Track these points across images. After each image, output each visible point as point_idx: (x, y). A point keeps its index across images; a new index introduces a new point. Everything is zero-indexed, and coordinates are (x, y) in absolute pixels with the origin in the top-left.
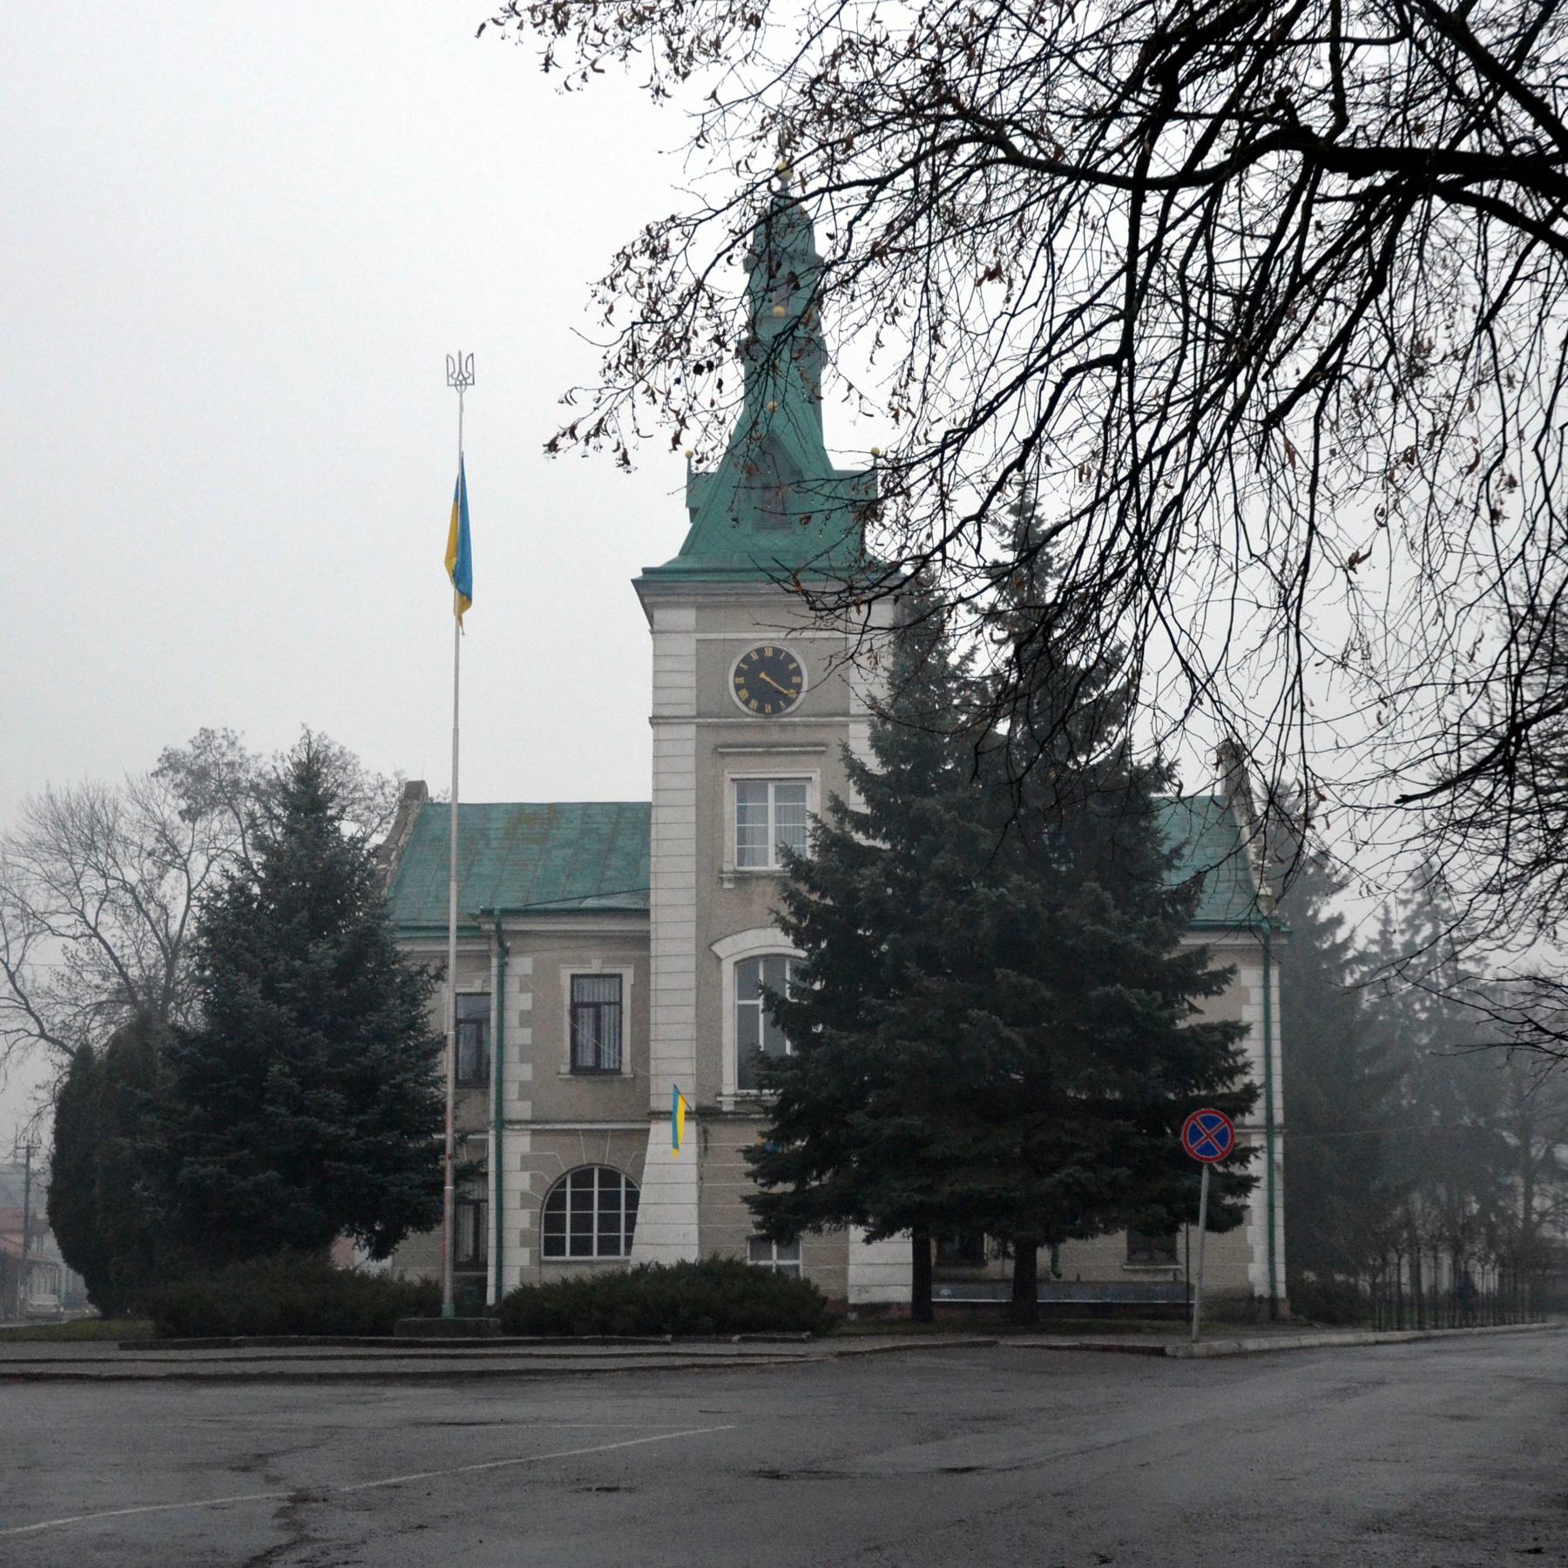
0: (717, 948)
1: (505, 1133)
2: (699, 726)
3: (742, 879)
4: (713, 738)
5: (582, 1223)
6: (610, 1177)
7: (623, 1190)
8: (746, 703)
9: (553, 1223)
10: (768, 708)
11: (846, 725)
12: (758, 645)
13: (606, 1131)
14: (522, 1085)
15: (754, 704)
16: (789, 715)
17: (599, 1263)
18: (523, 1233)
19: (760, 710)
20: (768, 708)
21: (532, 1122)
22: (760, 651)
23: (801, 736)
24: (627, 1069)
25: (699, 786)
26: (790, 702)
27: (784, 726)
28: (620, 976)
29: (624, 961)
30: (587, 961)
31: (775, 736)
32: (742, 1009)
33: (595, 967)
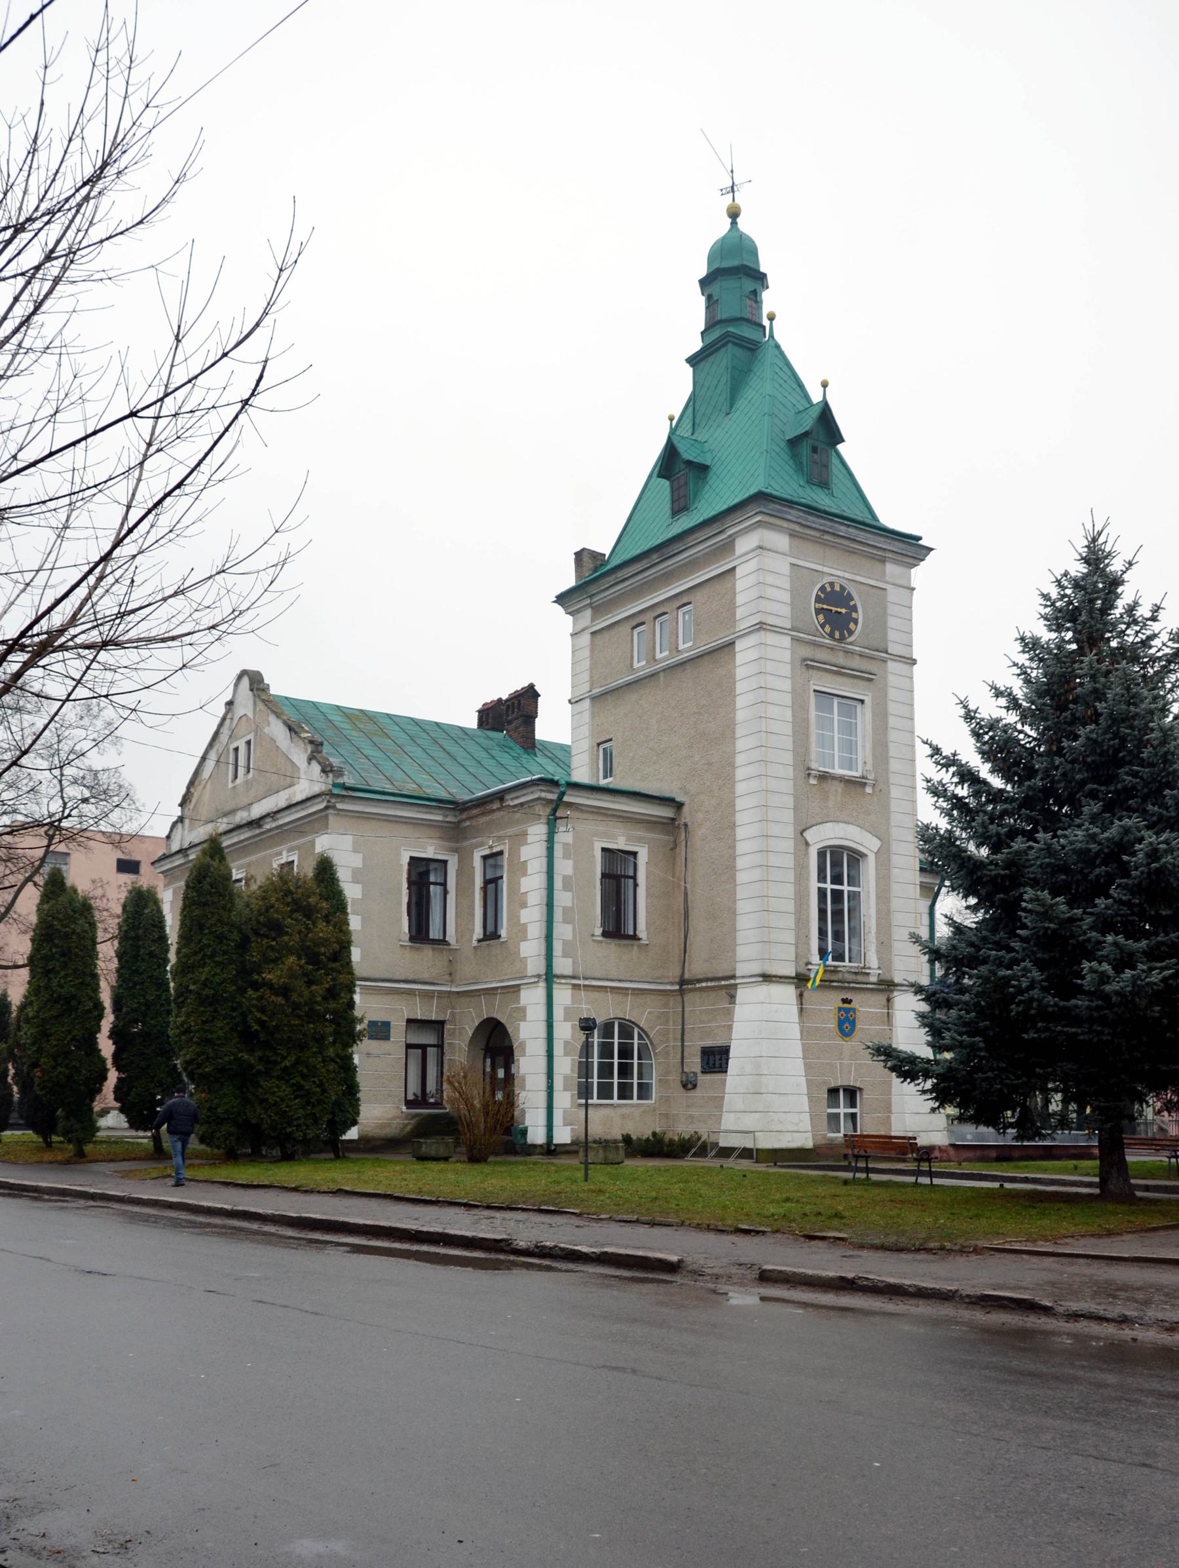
0: (808, 835)
1: (555, 986)
2: (794, 639)
3: (824, 777)
4: (807, 652)
5: (606, 1070)
6: (626, 1030)
7: (636, 1041)
8: (823, 626)
9: (585, 1069)
10: (837, 635)
11: (885, 661)
12: (831, 579)
13: (627, 989)
14: (565, 943)
15: (828, 628)
16: (851, 644)
17: (619, 1106)
18: (566, 1078)
19: (831, 635)
20: (837, 635)
21: (574, 977)
22: (832, 584)
23: (856, 663)
24: (642, 932)
25: (794, 691)
26: (851, 633)
27: (847, 652)
28: (635, 854)
29: (640, 840)
30: (613, 837)
31: (841, 659)
32: (819, 889)
33: (621, 844)
